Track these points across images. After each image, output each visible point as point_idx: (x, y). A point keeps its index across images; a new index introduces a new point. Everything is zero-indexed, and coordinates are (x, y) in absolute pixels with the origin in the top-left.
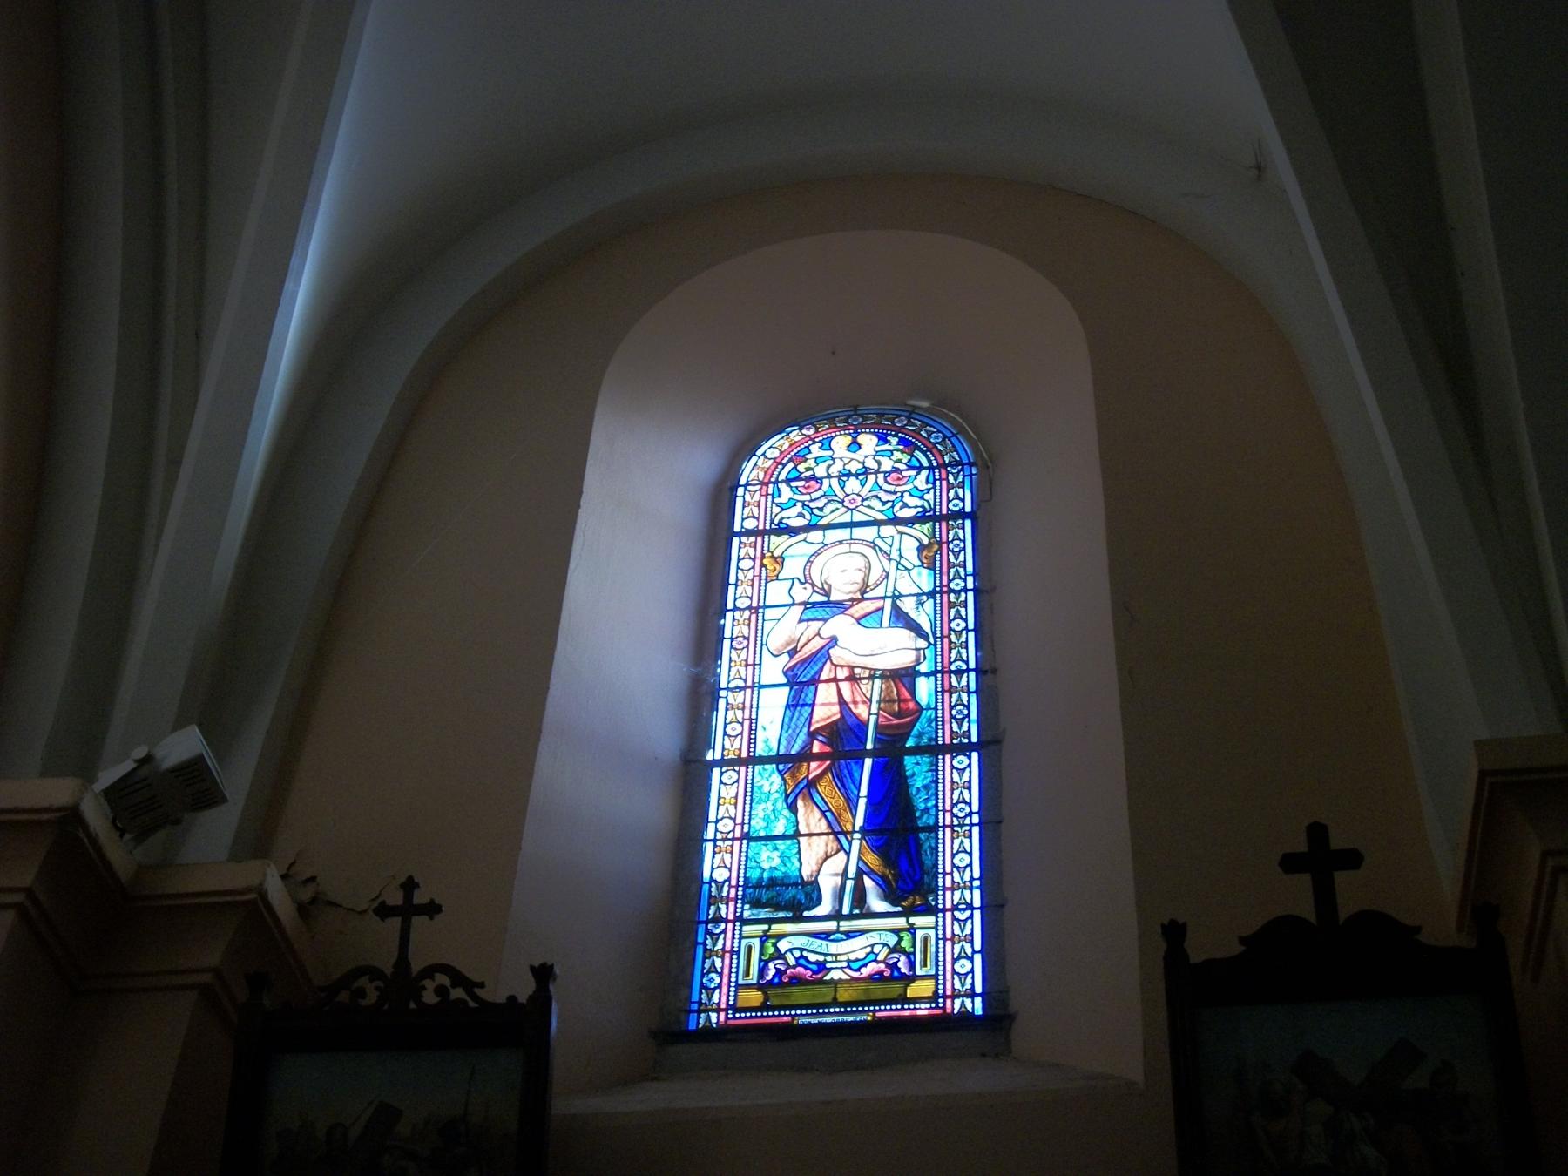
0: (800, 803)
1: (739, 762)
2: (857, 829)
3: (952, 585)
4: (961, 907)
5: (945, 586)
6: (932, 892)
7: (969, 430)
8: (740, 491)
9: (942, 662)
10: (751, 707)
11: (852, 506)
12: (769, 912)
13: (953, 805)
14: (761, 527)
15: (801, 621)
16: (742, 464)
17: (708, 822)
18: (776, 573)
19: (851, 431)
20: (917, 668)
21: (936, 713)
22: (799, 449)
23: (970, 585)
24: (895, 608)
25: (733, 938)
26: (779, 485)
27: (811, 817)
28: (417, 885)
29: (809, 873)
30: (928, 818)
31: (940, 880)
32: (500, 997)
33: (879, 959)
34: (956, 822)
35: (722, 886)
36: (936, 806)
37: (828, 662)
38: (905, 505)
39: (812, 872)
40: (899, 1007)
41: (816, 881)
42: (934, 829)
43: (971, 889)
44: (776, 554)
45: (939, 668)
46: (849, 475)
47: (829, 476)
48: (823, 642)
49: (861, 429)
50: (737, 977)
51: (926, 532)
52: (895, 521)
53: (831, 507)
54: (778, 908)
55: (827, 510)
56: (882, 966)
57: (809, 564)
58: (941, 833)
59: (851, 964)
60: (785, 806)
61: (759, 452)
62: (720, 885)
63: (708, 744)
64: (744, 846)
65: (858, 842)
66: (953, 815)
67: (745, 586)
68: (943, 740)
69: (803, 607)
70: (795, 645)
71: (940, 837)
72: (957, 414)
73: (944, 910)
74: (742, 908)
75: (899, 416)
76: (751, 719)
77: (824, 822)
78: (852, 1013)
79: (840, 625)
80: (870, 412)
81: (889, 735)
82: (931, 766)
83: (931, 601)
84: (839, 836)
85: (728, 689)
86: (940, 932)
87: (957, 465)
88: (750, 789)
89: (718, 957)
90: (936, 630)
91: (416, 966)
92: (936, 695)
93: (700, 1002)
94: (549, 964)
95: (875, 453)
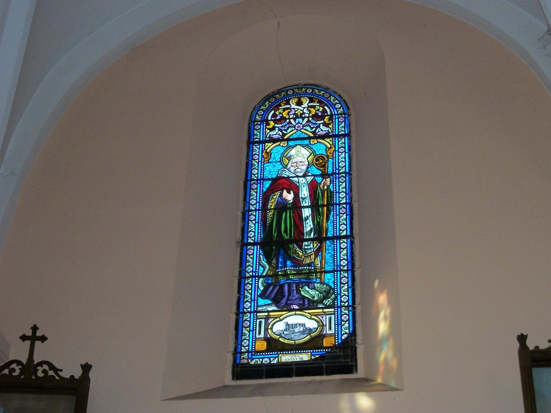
28: (38, 328)
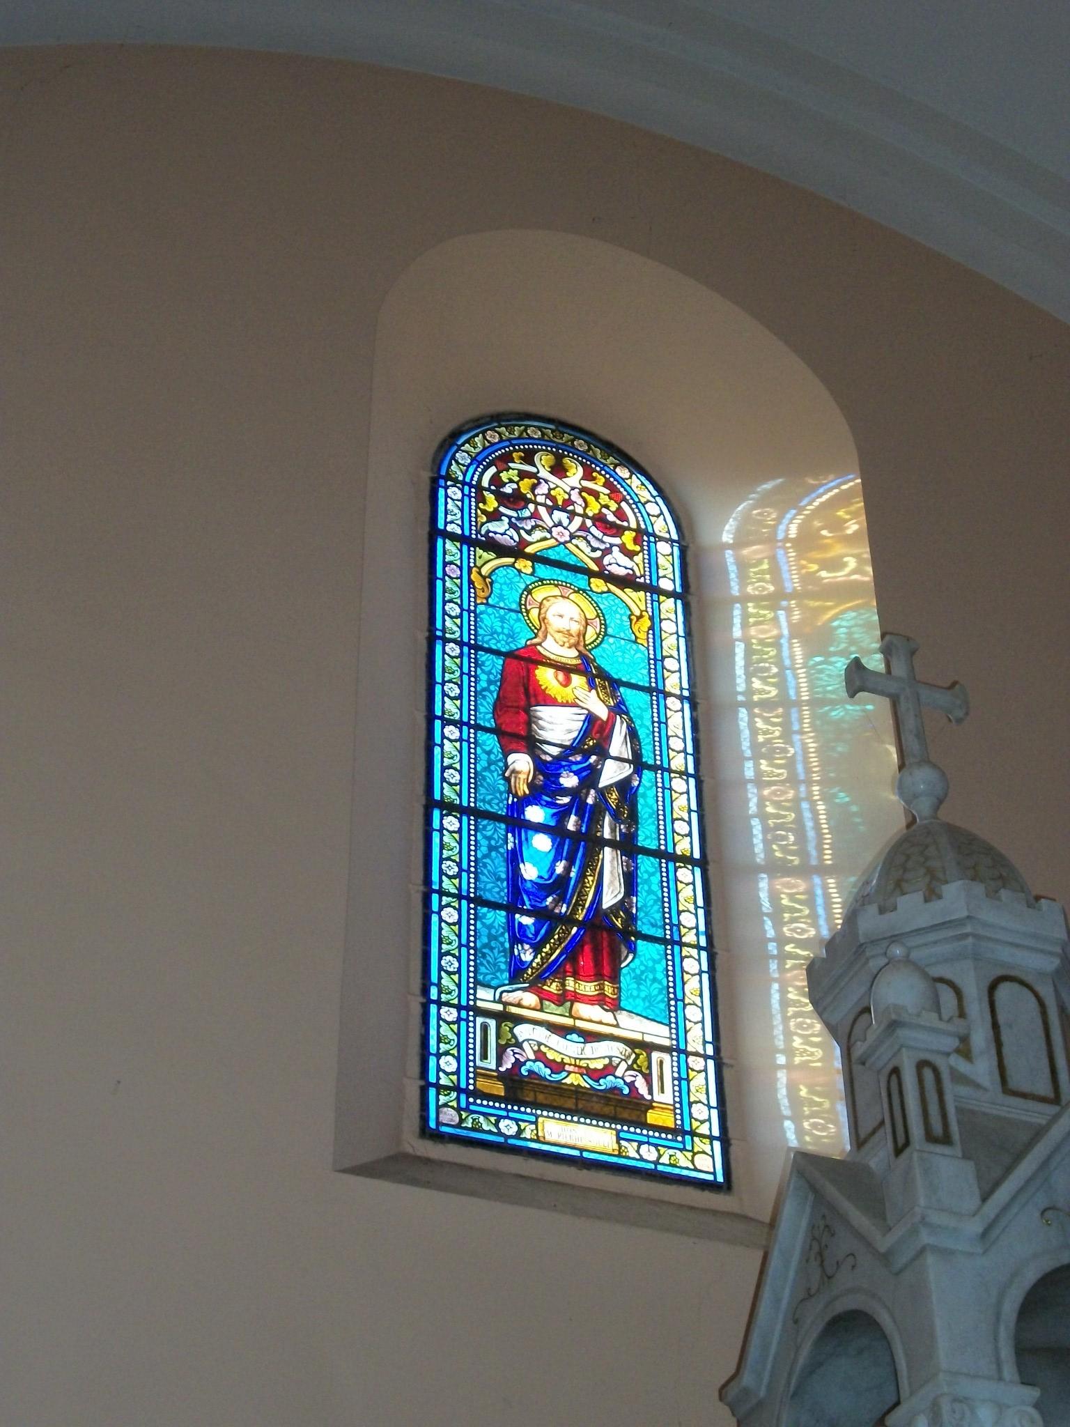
53: (538, 535)
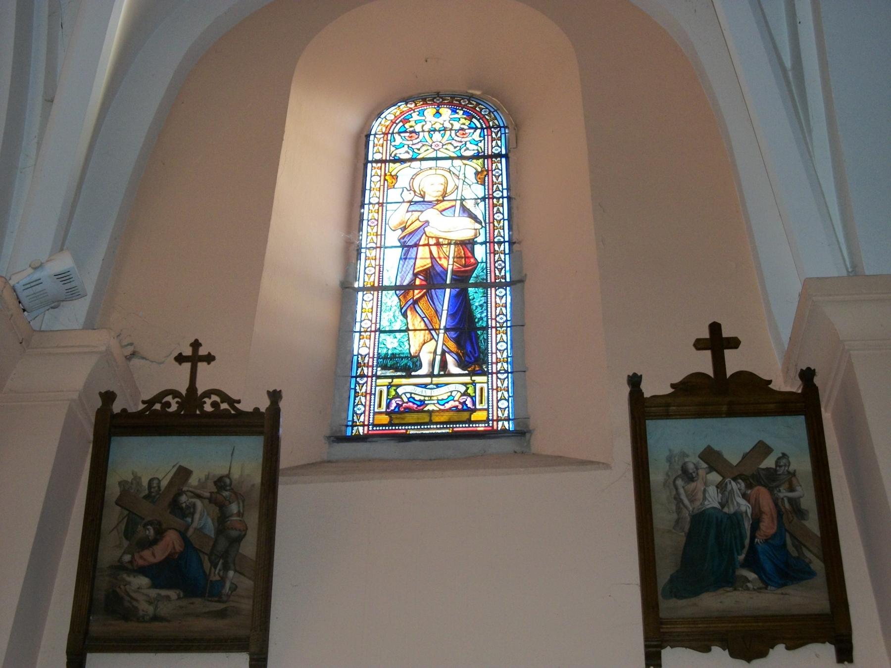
0: (409, 313)
1: (373, 288)
2: (442, 327)
3: (495, 195)
4: (501, 371)
5: (491, 195)
6: (485, 363)
7: (504, 108)
8: (372, 137)
9: (490, 237)
10: (380, 259)
11: (436, 149)
12: (392, 372)
13: (496, 316)
14: (384, 158)
15: (408, 211)
16: (373, 122)
17: (356, 322)
18: (393, 184)
19: (436, 106)
20: (475, 240)
21: (486, 265)
22: (405, 115)
23: (505, 195)
24: (462, 206)
25: (372, 386)
26: (394, 135)
27: (415, 320)
28: (200, 345)
29: (415, 351)
30: (482, 323)
31: (490, 357)
32: (249, 409)
33: (455, 399)
34: (498, 325)
35: (365, 358)
36: (487, 316)
37: (424, 235)
38: (467, 149)
39: (416, 350)
40: (467, 425)
41: (419, 356)
42: (485, 329)
43: (507, 362)
44: (393, 174)
45: (488, 240)
46: (435, 130)
47: (423, 131)
48: (421, 224)
49: (441, 105)
50: (374, 408)
51: (480, 164)
52: (462, 158)
53: (425, 148)
54: (397, 370)
55: (422, 150)
56: (457, 403)
57: (412, 180)
58: (490, 331)
59: (439, 401)
60: (400, 313)
61: (383, 116)
62: (363, 357)
63: (356, 279)
64: (377, 335)
65: (443, 335)
66: (496, 321)
67: (375, 191)
68: (491, 280)
69: (409, 204)
70: (405, 224)
71: (489, 333)
72: (497, 99)
73: (492, 373)
74: (377, 370)
75: (463, 99)
76: (380, 265)
77: (422, 323)
78: (440, 428)
79: (430, 214)
80: (447, 96)
81: (459, 276)
82: (484, 294)
83: (483, 203)
84: (432, 331)
85: (366, 248)
86: (490, 385)
87: (497, 128)
88: (380, 304)
89: (363, 396)
90: (486, 219)
91: (201, 389)
92: (486, 255)
93: (353, 421)
94: (278, 390)
95: (449, 119)
